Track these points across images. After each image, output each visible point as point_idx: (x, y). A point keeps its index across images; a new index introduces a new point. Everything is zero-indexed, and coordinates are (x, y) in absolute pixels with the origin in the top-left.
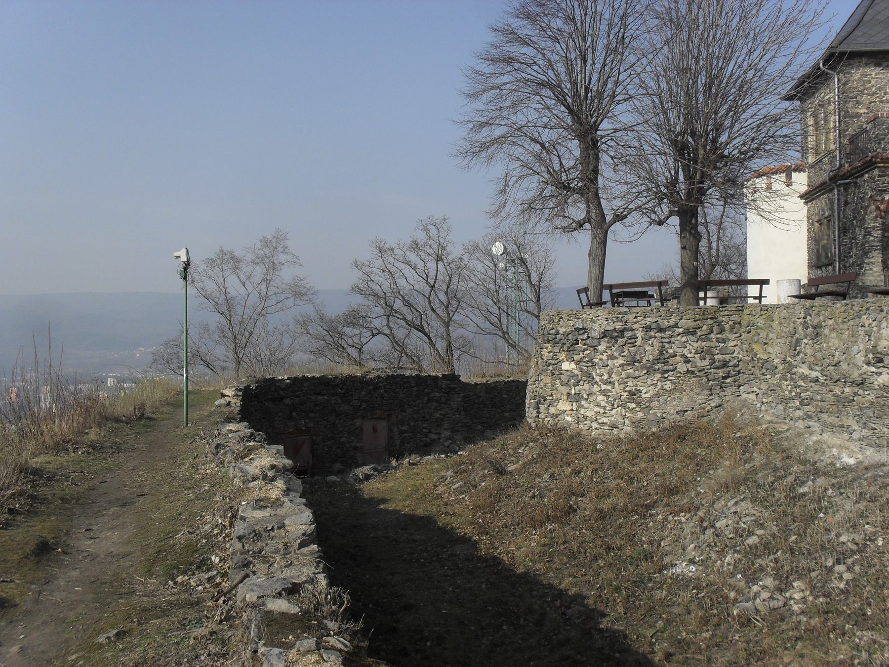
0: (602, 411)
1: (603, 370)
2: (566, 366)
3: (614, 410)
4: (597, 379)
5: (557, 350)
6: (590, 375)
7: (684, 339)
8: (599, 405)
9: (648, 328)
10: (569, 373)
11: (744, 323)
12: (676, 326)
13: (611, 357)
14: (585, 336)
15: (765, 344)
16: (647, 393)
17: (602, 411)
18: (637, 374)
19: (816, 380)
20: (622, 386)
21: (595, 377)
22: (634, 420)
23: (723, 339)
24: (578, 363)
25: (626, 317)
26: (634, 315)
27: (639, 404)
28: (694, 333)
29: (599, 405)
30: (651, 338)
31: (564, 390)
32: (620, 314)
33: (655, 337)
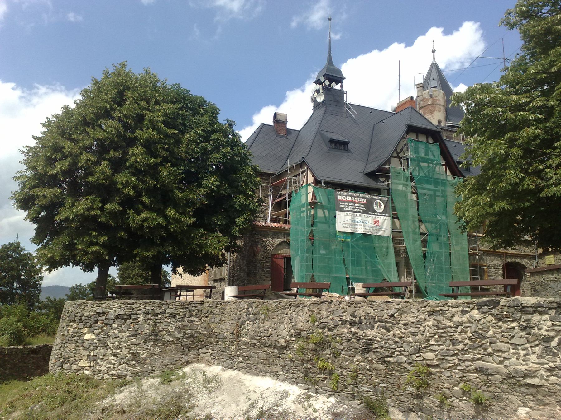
0: (112, 366)
1: (115, 340)
2: (87, 337)
3: (121, 366)
4: (111, 345)
5: (81, 326)
6: (105, 343)
7: (169, 320)
8: (110, 363)
9: (147, 313)
10: (89, 342)
11: (205, 311)
12: (164, 312)
13: (121, 331)
14: (104, 318)
15: (219, 323)
16: (144, 354)
17: (112, 366)
18: (138, 342)
19: (255, 345)
20: (127, 350)
21: (109, 344)
22: (134, 372)
23: (192, 321)
24: (97, 335)
25: (133, 306)
26: (139, 305)
27: (137, 361)
28: (175, 317)
29: (110, 363)
30: (148, 319)
31: (86, 353)
32: (129, 304)
33: (151, 319)
